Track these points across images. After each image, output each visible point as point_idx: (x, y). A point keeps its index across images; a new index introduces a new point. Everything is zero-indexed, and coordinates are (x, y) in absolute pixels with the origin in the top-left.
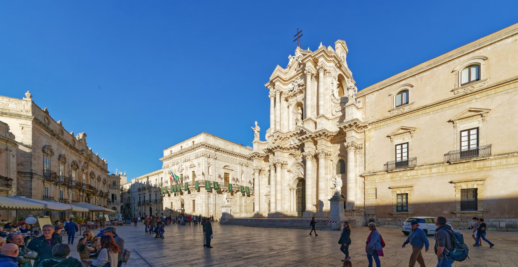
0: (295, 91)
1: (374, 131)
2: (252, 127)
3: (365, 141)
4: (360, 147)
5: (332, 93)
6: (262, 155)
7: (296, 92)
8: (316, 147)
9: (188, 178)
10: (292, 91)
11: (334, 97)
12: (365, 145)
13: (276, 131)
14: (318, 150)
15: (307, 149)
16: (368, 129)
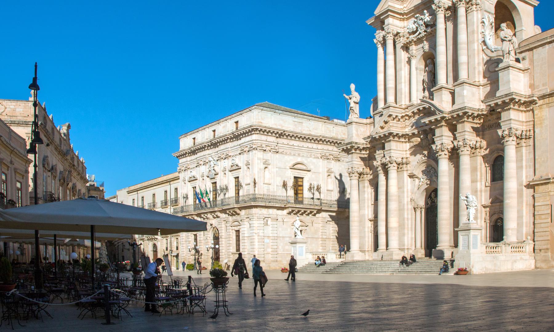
0: (420, 33)
1: (547, 109)
2: (345, 95)
3: (534, 125)
4: (526, 136)
5: (483, 39)
6: (363, 146)
7: (421, 35)
8: (454, 135)
9: (227, 189)
10: (414, 33)
11: (486, 47)
12: (534, 132)
13: (387, 105)
14: (458, 140)
15: (438, 139)
16: (537, 105)
